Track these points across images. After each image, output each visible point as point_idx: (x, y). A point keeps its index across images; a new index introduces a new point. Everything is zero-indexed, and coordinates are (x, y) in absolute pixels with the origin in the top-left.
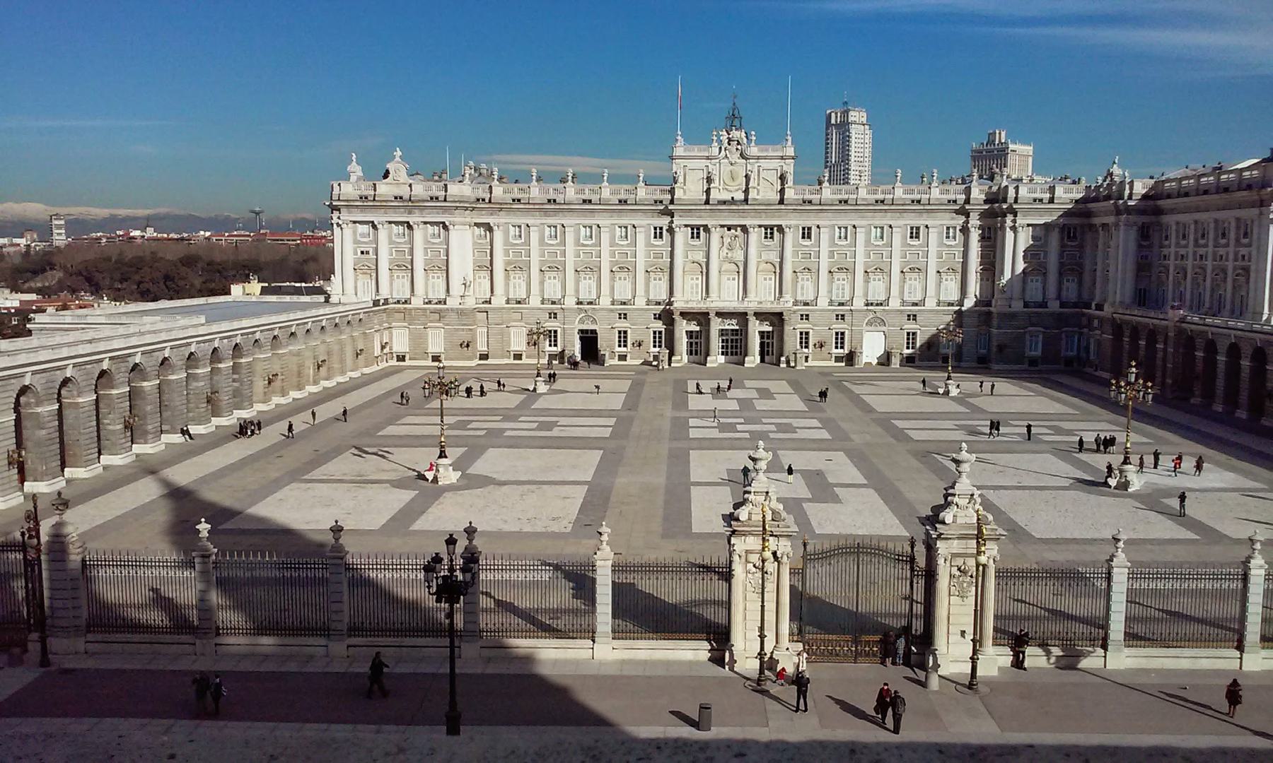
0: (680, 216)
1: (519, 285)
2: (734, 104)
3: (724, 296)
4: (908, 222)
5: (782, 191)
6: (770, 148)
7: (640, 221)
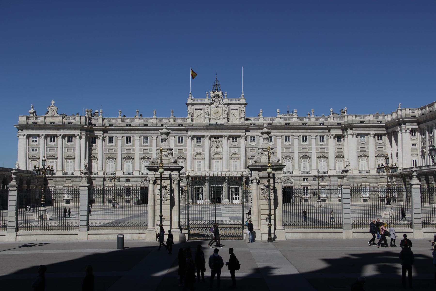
0: (191, 132)
1: (112, 166)
2: (217, 79)
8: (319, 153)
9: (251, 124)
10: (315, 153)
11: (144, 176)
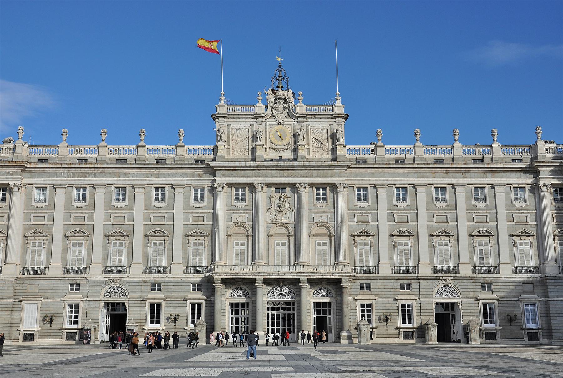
0: (223, 175)
3: (273, 261)
4: (471, 182)
5: (334, 150)
6: (319, 107)
7: (180, 181)
8: (514, 226)
9: (358, 161)
10: (506, 227)
11: (113, 275)
